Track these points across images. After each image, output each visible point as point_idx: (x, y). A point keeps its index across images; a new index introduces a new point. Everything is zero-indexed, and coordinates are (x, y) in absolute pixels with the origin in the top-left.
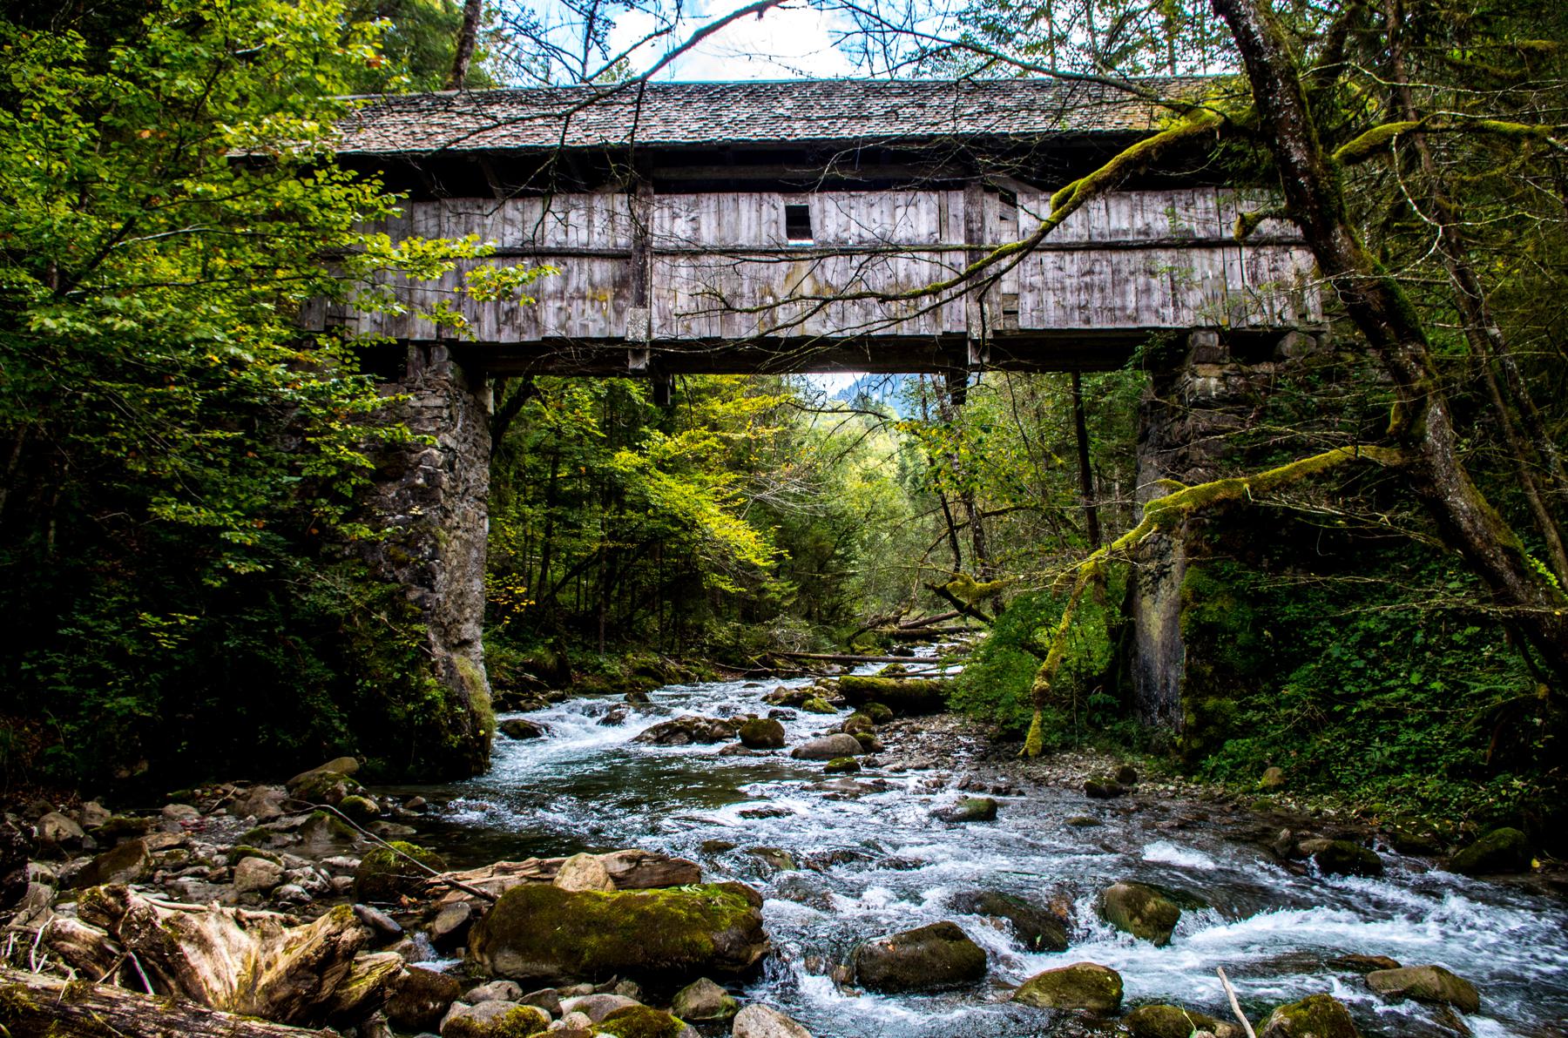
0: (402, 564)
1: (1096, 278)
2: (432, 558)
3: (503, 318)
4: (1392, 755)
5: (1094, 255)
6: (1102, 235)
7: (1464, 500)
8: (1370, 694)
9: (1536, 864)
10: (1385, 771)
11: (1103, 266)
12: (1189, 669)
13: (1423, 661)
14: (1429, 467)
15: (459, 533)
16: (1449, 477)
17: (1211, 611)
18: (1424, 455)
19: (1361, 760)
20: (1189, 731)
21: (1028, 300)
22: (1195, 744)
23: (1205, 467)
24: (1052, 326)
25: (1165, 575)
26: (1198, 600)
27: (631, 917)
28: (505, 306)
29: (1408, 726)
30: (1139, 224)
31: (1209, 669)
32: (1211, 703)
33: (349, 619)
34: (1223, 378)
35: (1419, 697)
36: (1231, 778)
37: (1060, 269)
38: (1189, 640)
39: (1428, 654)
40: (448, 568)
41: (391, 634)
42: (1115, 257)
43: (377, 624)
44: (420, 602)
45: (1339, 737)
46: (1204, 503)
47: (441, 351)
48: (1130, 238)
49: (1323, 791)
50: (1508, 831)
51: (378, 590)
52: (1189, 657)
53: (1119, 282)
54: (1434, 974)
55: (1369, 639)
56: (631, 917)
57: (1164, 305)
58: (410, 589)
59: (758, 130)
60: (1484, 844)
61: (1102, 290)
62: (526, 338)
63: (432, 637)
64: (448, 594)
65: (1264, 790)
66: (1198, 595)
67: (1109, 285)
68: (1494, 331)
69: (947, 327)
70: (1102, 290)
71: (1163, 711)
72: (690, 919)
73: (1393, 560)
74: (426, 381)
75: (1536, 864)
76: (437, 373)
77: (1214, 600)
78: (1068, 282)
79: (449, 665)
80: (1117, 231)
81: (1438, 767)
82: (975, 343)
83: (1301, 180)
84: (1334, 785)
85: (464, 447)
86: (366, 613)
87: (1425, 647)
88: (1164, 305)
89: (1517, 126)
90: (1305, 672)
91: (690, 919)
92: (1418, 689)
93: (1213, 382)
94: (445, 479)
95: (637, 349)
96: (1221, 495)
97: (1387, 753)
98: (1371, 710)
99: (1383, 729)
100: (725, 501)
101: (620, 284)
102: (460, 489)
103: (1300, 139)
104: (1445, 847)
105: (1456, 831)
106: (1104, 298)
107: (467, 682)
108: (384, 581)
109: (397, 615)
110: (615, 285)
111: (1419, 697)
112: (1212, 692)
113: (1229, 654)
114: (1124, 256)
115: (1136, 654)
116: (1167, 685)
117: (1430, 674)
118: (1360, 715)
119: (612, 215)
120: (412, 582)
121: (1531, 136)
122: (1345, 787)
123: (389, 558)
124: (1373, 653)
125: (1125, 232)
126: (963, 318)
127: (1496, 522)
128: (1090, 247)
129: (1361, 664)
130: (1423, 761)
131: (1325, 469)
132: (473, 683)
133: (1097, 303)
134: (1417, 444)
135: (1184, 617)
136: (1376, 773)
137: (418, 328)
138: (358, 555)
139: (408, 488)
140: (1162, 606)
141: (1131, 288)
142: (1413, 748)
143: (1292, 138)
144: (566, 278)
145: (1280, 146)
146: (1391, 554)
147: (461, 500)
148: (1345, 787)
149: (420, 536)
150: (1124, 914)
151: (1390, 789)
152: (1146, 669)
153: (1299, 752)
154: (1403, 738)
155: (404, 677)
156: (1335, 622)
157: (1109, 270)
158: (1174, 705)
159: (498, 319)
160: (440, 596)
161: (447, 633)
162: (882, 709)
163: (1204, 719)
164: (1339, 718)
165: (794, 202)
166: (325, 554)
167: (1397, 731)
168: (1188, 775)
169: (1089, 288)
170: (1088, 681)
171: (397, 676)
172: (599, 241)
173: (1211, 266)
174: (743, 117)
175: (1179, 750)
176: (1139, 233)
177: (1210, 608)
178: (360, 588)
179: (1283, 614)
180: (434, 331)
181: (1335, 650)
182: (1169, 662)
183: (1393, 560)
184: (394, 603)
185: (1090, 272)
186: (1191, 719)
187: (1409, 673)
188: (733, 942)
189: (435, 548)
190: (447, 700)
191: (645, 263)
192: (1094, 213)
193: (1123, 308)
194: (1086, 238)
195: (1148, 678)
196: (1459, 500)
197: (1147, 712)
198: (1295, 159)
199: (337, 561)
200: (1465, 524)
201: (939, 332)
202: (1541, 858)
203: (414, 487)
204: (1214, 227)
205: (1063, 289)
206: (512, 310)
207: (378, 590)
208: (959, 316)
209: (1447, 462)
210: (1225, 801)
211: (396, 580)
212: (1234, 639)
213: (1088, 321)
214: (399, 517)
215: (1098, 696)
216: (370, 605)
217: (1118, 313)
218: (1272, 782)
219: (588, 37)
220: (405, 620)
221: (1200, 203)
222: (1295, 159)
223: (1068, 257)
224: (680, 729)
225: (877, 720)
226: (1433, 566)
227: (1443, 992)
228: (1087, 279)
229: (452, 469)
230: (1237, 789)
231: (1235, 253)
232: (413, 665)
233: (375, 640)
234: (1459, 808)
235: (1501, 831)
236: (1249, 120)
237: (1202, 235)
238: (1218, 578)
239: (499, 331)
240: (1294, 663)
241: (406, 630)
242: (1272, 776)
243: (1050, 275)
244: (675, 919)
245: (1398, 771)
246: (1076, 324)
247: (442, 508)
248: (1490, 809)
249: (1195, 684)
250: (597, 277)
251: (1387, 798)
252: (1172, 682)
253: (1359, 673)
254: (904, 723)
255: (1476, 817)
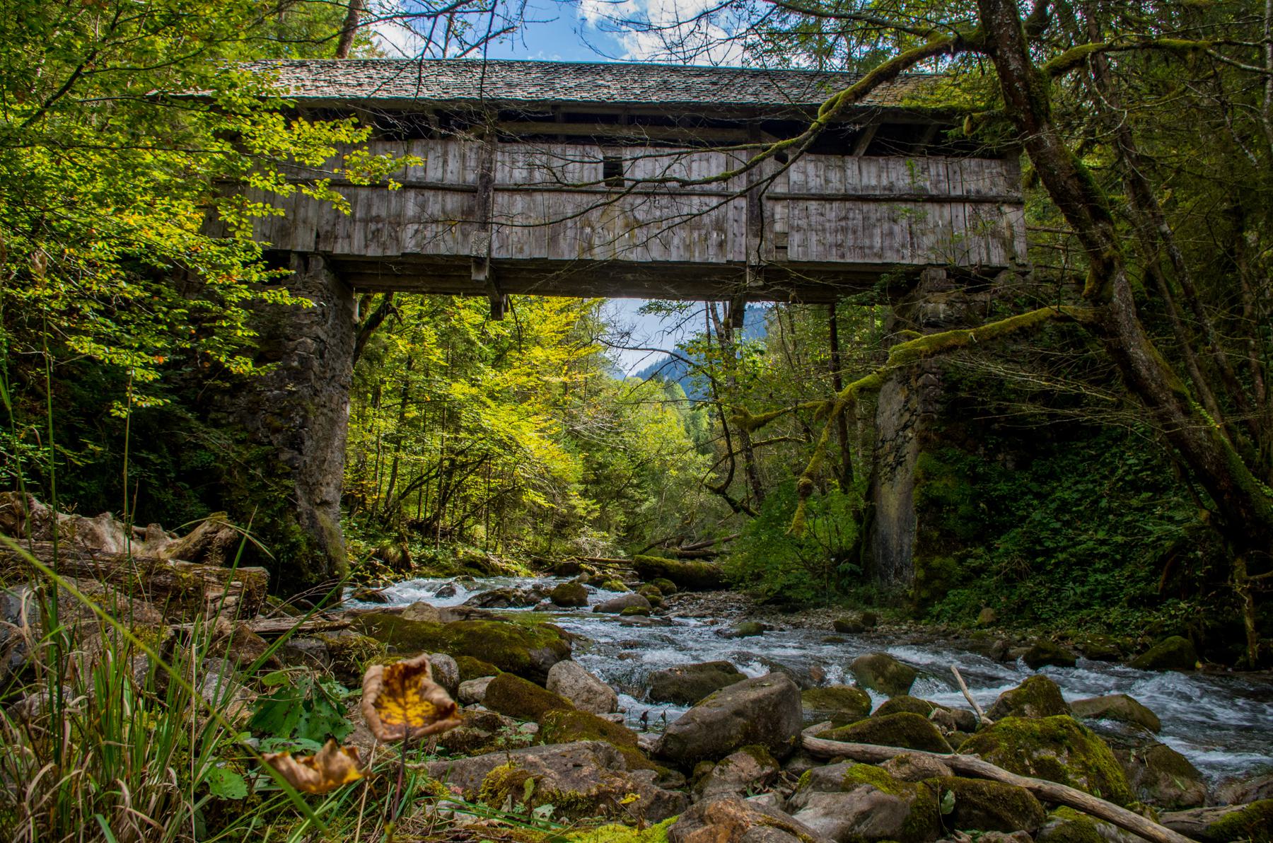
0: (277, 430)
1: (850, 223)
2: (302, 427)
3: (370, 236)
4: (1082, 594)
5: (849, 205)
6: (855, 189)
7: (1143, 351)
8: (1064, 549)
9: (1199, 665)
10: (1078, 606)
11: (857, 214)
12: (919, 534)
13: (1107, 522)
14: (1115, 323)
15: (325, 411)
16: (1131, 333)
17: (938, 487)
18: (1111, 314)
19: (1058, 600)
20: (921, 584)
21: (796, 238)
22: (924, 594)
23: (935, 374)
24: (814, 258)
25: (900, 464)
26: (927, 479)
27: (461, 636)
28: (373, 226)
29: (1095, 571)
30: (885, 182)
31: (936, 534)
32: (936, 561)
33: (230, 473)
34: (950, 304)
35: (1104, 549)
36: (953, 619)
37: (822, 215)
38: (921, 510)
39: (1111, 517)
40: (315, 437)
41: (265, 487)
42: (865, 207)
43: (252, 478)
44: (289, 462)
45: (1040, 583)
46: (938, 348)
47: (317, 261)
48: (877, 193)
49: (1027, 625)
50: (1178, 638)
51: (255, 451)
52: (919, 524)
53: (868, 227)
54: (1124, 700)
55: (1064, 506)
56: (461, 636)
57: (903, 246)
58: (283, 451)
59: (584, 95)
60: (1158, 649)
61: (855, 232)
62: (389, 253)
63: (299, 492)
64: (314, 459)
65: (980, 627)
66: (928, 475)
67: (860, 229)
68: (1165, 228)
69: (730, 257)
70: (855, 232)
71: (898, 573)
72: (511, 637)
73: (1083, 448)
74: (304, 283)
75: (1199, 665)
76: (316, 276)
77: (940, 479)
78: (827, 225)
79: (312, 517)
80: (867, 187)
81: (1120, 600)
82: (752, 267)
83: (1017, 85)
84: (1036, 620)
85: (332, 342)
86: (244, 468)
87: (1110, 511)
88: (903, 246)
89: (1184, 42)
90: (1013, 534)
91: (511, 637)
92: (1103, 542)
93: (942, 307)
94: (316, 363)
95: (479, 262)
96: (951, 342)
97: (1078, 591)
98: (1066, 560)
99: (1075, 573)
100: (541, 431)
101: (468, 213)
102: (328, 375)
103: (1016, 51)
104: (1126, 655)
105: (1135, 644)
106: (856, 239)
107: (326, 533)
108: (260, 444)
109: (270, 473)
110: (463, 213)
111: (1104, 549)
112: (938, 553)
113: (952, 522)
114: (872, 206)
115: (876, 531)
116: (901, 551)
117: (1113, 529)
118: (1057, 565)
119: (463, 157)
120: (284, 445)
121: (1195, 49)
122: (1045, 620)
123: (267, 426)
124: (1067, 517)
125: (874, 188)
126: (744, 250)
127: (1168, 372)
128: (845, 198)
129: (1058, 525)
130: (1108, 599)
131: (1034, 324)
132: (331, 534)
133: (850, 242)
134: (1106, 304)
135: (915, 491)
136: (1070, 609)
137: (300, 241)
138: (240, 422)
139: (284, 369)
140: (899, 488)
141: (877, 231)
142: (1100, 588)
143: (1010, 50)
144: (423, 207)
145: (1001, 57)
146: (1081, 444)
147: (328, 384)
148: (1045, 620)
149: (293, 408)
150: (870, 676)
151: (1082, 619)
152: (884, 543)
153: (1008, 598)
154: (1092, 579)
155: (273, 522)
156: (1038, 496)
157: (860, 217)
158: (907, 566)
159: (366, 237)
160: (307, 459)
161: (311, 492)
162: (669, 584)
163: (932, 574)
164: (1039, 568)
165: (610, 154)
166: (213, 420)
167: (1086, 576)
168: (918, 618)
169: (844, 230)
170: (840, 556)
171: (268, 520)
172: (452, 178)
173: (941, 217)
174: (572, 85)
175: (911, 600)
176: (885, 189)
177: (937, 484)
178: (241, 448)
179: (995, 490)
180: (312, 245)
181: (1036, 516)
182: (903, 531)
183: (1083, 448)
184: (269, 463)
185: (846, 218)
186: (921, 574)
187: (1096, 531)
188: (546, 659)
189: (305, 418)
190: (309, 544)
191: (488, 196)
192: (849, 172)
193: (871, 247)
194: (843, 191)
195: (886, 548)
196: (1139, 351)
197: (884, 576)
198: (1012, 67)
199: (223, 426)
200: (1144, 372)
201: (724, 261)
202: (1203, 662)
203: (290, 369)
204: (944, 186)
205: (824, 230)
206: (378, 230)
207: (255, 451)
208: (740, 248)
209: (1130, 320)
210: (949, 634)
211: (270, 443)
212: (955, 510)
213: (843, 256)
214: (276, 392)
215: (845, 566)
216: (248, 462)
217: (867, 251)
218: (986, 620)
219: (448, 30)
220: (279, 476)
221: (933, 171)
222: (1012, 67)
223: (828, 206)
224: (501, 597)
225: (666, 592)
226: (1114, 450)
227: (1131, 714)
228: (843, 223)
229: (322, 356)
230: (959, 627)
231: (960, 207)
232: (281, 513)
233: (252, 491)
234: (1137, 628)
235: (1172, 638)
236: (977, 36)
237: (934, 192)
238: (944, 462)
239: (366, 246)
240: (1001, 530)
241: (276, 483)
242: (986, 615)
243: (813, 219)
244: (498, 638)
245: (1088, 605)
246: (834, 258)
247: (312, 387)
248: (1162, 625)
249: (924, 545)
250: (449, 206)
251: (1079, 626)
252: (906, 548)
253: (1056, 532)
254: (686, 595)
255: (1150, 633)
